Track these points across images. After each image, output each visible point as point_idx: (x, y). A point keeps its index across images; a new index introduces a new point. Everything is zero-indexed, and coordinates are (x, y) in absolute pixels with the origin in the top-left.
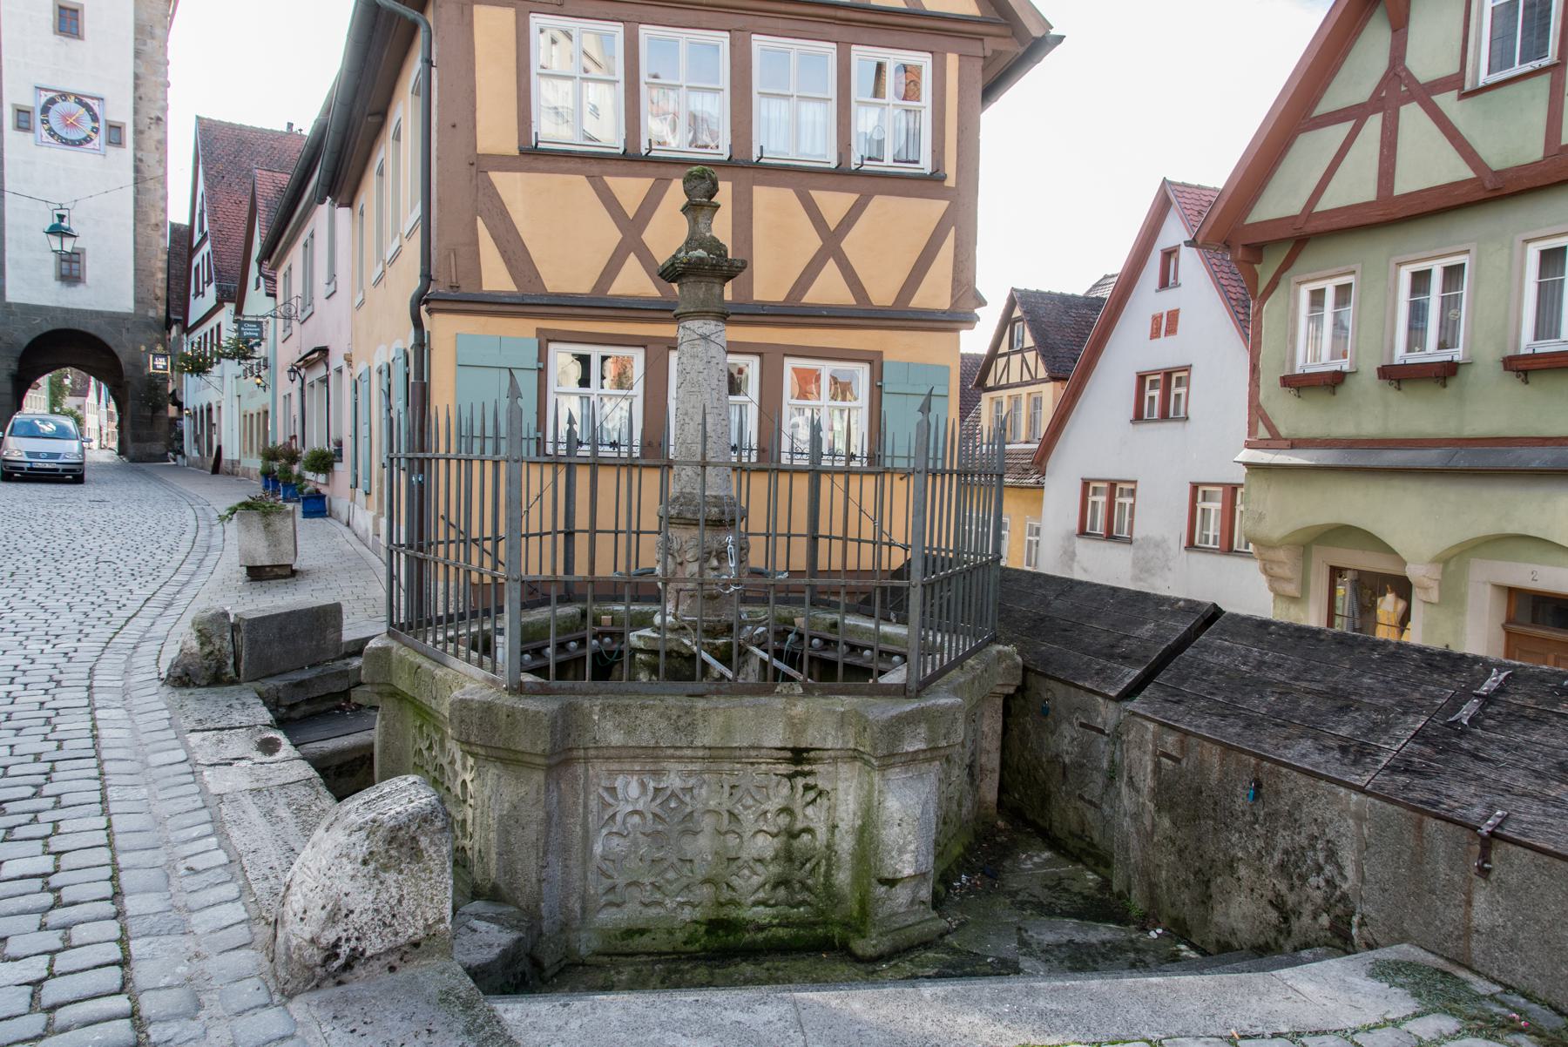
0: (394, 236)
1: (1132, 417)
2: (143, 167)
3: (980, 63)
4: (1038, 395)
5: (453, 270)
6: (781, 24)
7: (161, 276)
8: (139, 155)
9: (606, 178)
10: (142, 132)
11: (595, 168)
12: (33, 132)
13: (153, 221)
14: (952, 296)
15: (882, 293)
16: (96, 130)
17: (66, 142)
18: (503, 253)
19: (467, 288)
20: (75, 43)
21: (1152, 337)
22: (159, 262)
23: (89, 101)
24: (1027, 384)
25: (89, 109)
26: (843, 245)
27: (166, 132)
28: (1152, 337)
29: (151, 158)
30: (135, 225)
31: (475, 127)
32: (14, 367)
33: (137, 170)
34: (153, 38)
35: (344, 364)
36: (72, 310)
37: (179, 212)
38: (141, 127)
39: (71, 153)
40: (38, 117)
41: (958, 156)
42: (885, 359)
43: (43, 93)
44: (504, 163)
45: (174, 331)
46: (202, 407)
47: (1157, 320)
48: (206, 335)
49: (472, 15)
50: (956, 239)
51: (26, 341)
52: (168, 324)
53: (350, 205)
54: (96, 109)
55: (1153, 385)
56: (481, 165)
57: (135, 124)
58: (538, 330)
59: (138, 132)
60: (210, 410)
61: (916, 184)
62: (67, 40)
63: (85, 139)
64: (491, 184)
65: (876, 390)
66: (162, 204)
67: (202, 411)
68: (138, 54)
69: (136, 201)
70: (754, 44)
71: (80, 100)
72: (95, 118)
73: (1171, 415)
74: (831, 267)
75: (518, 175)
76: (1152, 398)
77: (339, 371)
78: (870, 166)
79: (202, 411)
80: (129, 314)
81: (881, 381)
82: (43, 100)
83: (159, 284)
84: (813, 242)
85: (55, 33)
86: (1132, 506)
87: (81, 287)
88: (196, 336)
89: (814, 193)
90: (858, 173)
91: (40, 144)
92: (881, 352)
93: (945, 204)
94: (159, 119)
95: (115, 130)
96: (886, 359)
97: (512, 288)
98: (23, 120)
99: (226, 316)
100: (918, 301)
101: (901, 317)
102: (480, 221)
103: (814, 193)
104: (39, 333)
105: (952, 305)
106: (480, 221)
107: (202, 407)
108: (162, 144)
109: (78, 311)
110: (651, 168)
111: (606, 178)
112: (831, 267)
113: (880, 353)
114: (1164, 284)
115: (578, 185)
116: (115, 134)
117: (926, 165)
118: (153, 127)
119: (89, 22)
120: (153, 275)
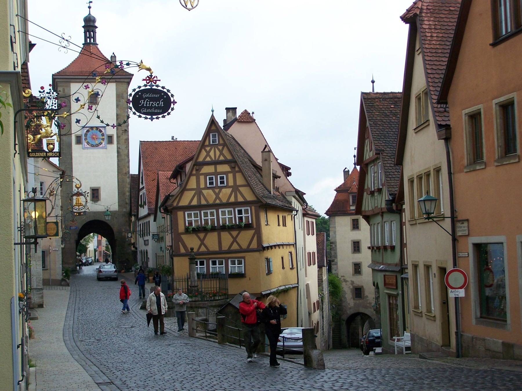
2: (120, 150)
3: (258, 207)
7: (128, 194)
8: (119, 146)
12: (82, 144)
13: (124, 172)
15: (244, 246)
17: (93, 146)
22: (127, 189)
23: (101, 129)
25: (101, 131)
26: (237, 240)
27: (128, 135)
29: (123, 147)
30: (118, 174)
32: (77, 237)
34: (123, 99)
36: (96, 212)
37: (134, 170)
38: (119, 135)
39: (95, 151)
40: (83, 138)
43: (85, 129)
44: (183, 234)
45: (133, 219)
46: (144, 250)
48: (145, 223)
51: (80, 227)
52: (130, 215)
54: (103, 130)
59: (118, 137)
60: (147, 252)
63: (100, 143)
64: (181, 237)
66: (127, 164)
67: (144, 252)
68: (117, 106)
71: (97, 128)
74: (235, 243)
79: (144, 252)
80: (116, 211)
82: (85, 131)
83: (127, 197)
84: (232, 240)
87: (99, 203)
88: (141, 222)
91: (84, 148)
94: (126, 130)
95: (110, 138)
97: (185, 252)
98: (79, 140)
99: (152, 218)
101: (249, 250)
104: (85, 222)
107: (144, 250)
108: (127, 140)
109: (98, 212)
112: (235, 243)
113: (245, 257)
116: (110, 139)
118: (123, 134)
120: (124, 194)
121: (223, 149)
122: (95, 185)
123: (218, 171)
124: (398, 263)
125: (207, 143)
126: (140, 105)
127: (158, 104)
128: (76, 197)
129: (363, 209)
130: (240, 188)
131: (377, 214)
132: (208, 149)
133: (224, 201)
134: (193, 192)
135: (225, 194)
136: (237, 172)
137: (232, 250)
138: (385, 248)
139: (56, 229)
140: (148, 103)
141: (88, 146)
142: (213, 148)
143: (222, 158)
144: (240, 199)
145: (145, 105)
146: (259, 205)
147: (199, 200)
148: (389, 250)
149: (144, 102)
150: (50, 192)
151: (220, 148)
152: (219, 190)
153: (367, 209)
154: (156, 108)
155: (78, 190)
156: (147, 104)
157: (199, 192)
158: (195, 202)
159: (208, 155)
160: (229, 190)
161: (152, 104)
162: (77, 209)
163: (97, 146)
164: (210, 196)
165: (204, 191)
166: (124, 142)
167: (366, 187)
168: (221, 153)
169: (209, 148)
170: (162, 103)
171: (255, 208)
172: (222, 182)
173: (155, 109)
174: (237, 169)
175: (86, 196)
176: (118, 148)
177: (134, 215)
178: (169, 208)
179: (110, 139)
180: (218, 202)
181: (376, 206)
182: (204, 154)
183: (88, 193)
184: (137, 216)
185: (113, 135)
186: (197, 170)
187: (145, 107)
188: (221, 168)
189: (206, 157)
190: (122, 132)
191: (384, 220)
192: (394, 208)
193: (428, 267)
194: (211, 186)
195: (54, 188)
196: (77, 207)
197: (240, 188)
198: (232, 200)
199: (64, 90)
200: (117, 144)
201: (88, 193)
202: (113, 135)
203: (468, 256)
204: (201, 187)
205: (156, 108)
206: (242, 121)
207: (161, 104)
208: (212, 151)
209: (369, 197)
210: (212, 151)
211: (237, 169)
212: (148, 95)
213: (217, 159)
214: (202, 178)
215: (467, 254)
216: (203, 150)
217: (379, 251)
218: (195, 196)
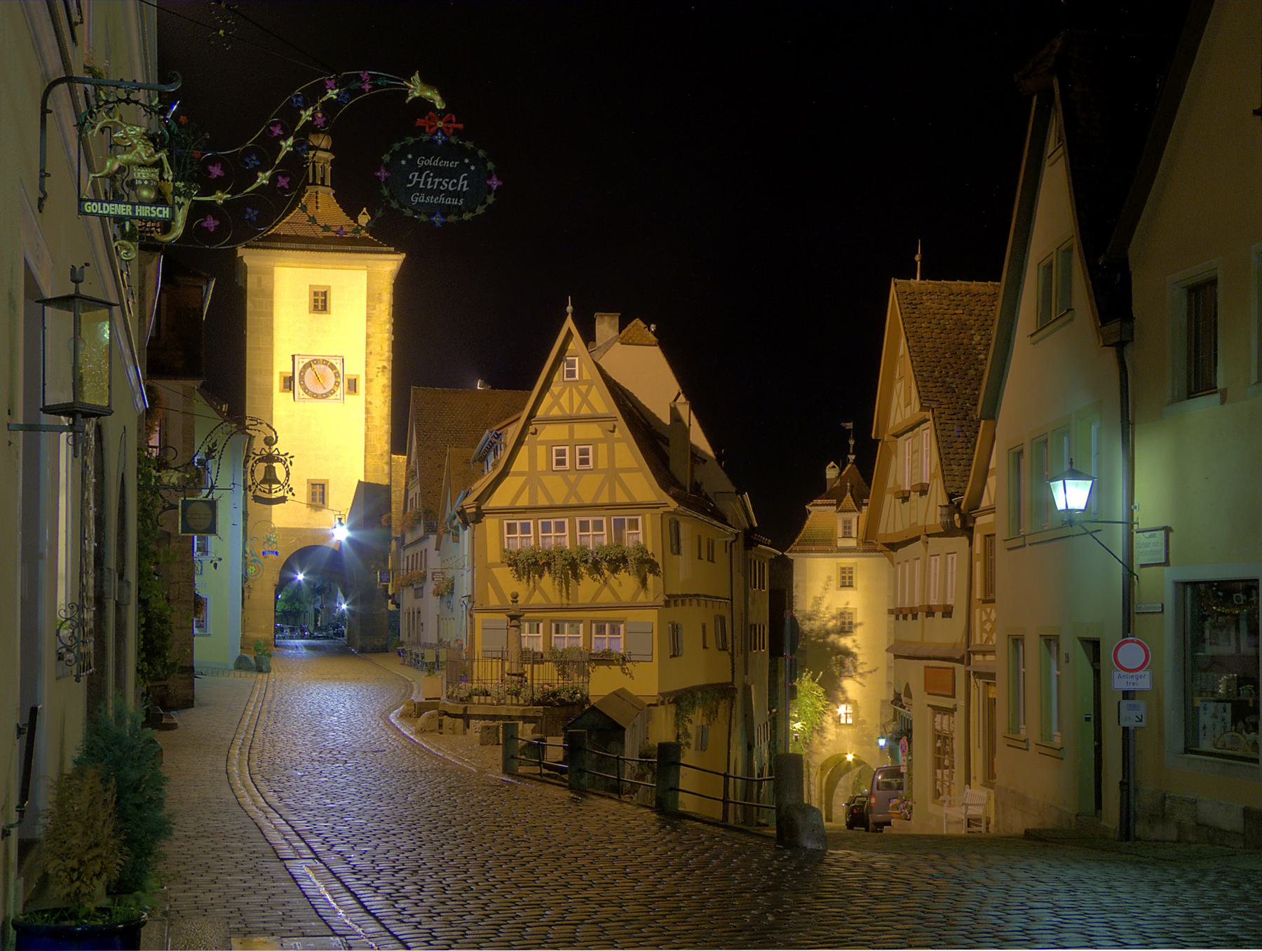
2: (372, 408)
10: (371, 380)
16: (337, 384)
17: (315, 396)
20: (322, 317)
25: (333, 367)
30: (365, 456)
33: (367, 411)
38: (370, 377)
44: (495, 565)
56: (489, 567)
57: (366, 375)
59: (368, 381)
62: (317, 315)
63: (329, 392)
64: (492, 573)
68: (369, 317)
69: (366, 435)
72: (337, 375)
85: (310, 312)
87: (325, 511)
88: (409, 552)
92: (626, 618)
96: (629, 620)
98: (289, 383)
102: (489, 584)
106: (489, 584)
119: (333, 302)
121: (588, 391)
122: (318, 476)
123: (575, 438)
124: (959, 641)
125: (556, 378)
126: (408, 185)
127: (454, 185)
128: (266, 465)
129: (881, 530)
131: (917, 539)
132: (555, 389)
133: (587, 501)
135: (589, 489)
136: (618, 440)
138: (930, 612)
139: (211, 516)
140: (430, 180)
141: (306, 396)
142: (568, 390)
143: (585, 411)
144: (621, 498)
145: (421, 186)
146: (661, 510)
147: (533, 495)
148: (939, 614)
149: (420, 177)
150: (207, 451)
151: (583, 388)
152: (575, 476)
153: (890, 531)
154: (448, 194)
155: (270, 448)
156: (425, 183)
157: (533, 478)
158: (523, 501)
159: (556, 402)
160: (597, 479)
161: (440, 184)
162: (267, 491)
163: (325, 396)
164: (557, 491)
166: (380, 391)
167: (890, 484)
168: (585, 398)
170: (466, 182)
172: (584, 462)
173: (445, 197)
175: (288, 463)
176: (368, 403)
177: (396, 539)
178: (468, 511)
179: (353, 386)
180: (573, 501)
181: (912, 522)
182: (548, 399)
183: (292, 457)
184: (401, 541)
185: (358, 376)
187: (421, 191)
188: (585, 431)
189: (551, 408)
190: (377, 370)
191: (930, 551)
192: (958, 524)
193: (1050, 641)
194: (560, 468)
195: (217, 443)
196: (267, 486)
197: (622, 475)
198: (605, 499)
199: (259, 281)
200: (366, 394)
201: (292, 457)
202: (358, 376)
203: (1162, 611)
204: (539, 469)
205: (448, 194)
206: (630, 341)
207: (463, 185)
209: (897, 504)
211: (617, 434)
212: (430, 162)
213: (574, 412)
214: (541, 451)
215: (1160, 605)
217: (915, 617)
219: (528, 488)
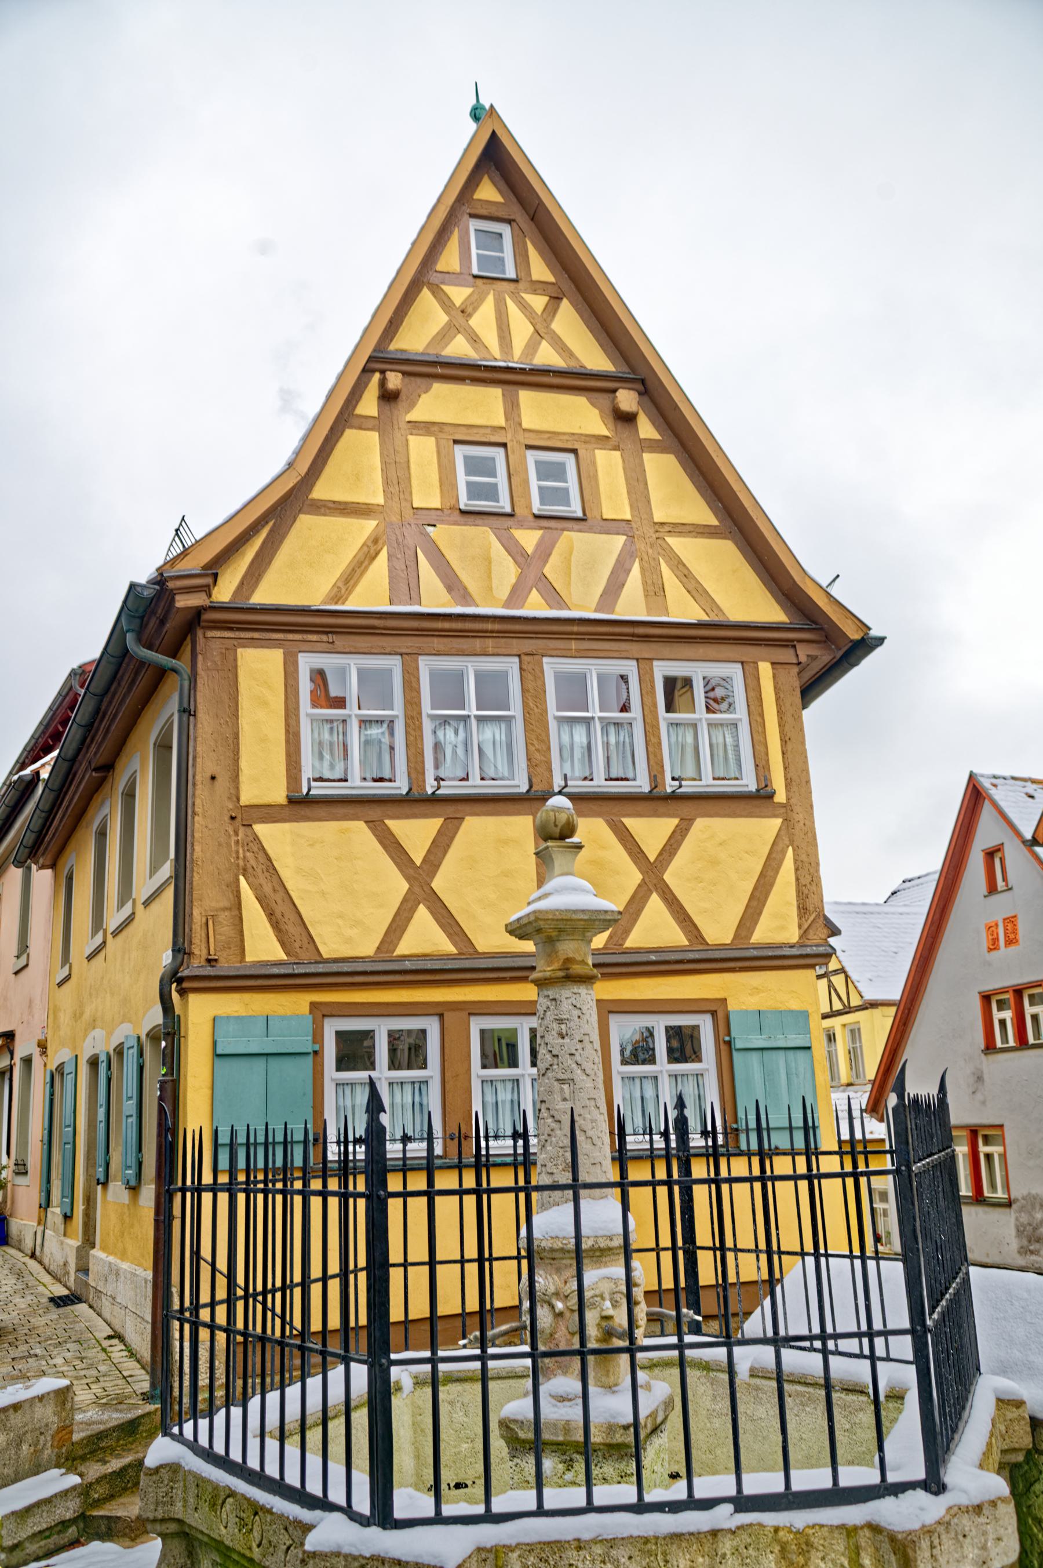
0: (121, 904)
1: (983, 1047)
3: (795, 670)
4: (856, 1027)
5: (211, 940)
6: (574, 645)
9: (387, 822)
11: (375, 812)
14: (800, 927)
18: (270, 915)
19: (227, 964)
21: (990, 950)
24: (839, 1013)
28: (990, 950)
31: (237, 776)
35: (36, 1052)
41: (785, 768)
42: (729, 1008)
44: (268, 813)
47: (991, 928)
49: (235, 660)
50: (795, 861)
53: (53, 866)
55: (1002, 1005)
58: (314, 1006)
61: (741, 805)
64: (256, 838)
65: (723, 1047)
70: (545, 666)
73: (1031, 1040)
74: (655, 902)
75: (286, 826)
76: (1003, 1023)
77: (27, 1061)
78: (689, 787)
81: (729, 1034)
86: (1003, 1157)
89: (628, 822)
90: (675, 797)
93: (778, 821)
100: (762, 934)
103: (628, 822)
105: (801, 937)
110: (438, 808)
111: (391, 823)
112: (655, 902)
114: (992, 889)
115: (358, 831)
117: (749, 783)
125: (449, 260)
130: (670, 540)
134: (369, 526)
136: (652, 446)
137: (637, 951)
142: (490, 300)
143: (547, 356)
165: (440, 534)
168: (542, 331)
169: (467, 291)
171: (774, 676)
174: (646, 429)
180: (535, 607)
186: (388, 397)
189: (445, 335)
208: (487, 310)
210: (487, 310)
216: (426, 293)
218: (377, 554)
219: (384, 554)
